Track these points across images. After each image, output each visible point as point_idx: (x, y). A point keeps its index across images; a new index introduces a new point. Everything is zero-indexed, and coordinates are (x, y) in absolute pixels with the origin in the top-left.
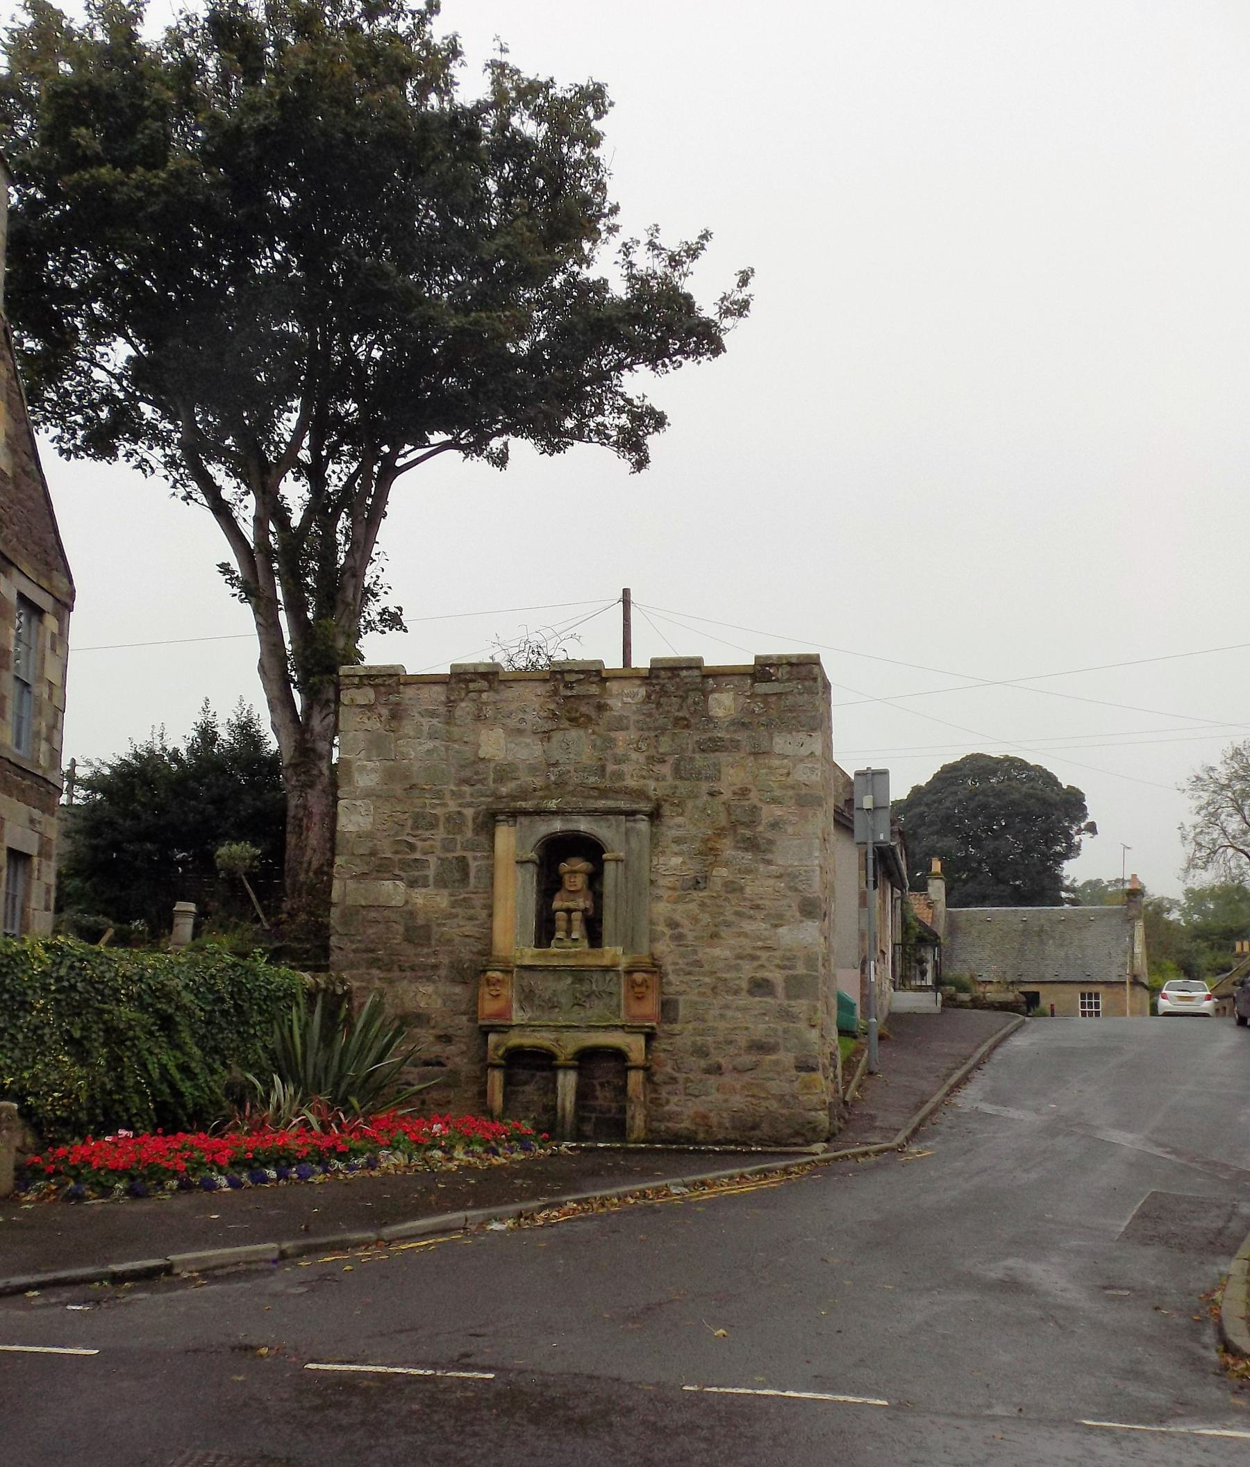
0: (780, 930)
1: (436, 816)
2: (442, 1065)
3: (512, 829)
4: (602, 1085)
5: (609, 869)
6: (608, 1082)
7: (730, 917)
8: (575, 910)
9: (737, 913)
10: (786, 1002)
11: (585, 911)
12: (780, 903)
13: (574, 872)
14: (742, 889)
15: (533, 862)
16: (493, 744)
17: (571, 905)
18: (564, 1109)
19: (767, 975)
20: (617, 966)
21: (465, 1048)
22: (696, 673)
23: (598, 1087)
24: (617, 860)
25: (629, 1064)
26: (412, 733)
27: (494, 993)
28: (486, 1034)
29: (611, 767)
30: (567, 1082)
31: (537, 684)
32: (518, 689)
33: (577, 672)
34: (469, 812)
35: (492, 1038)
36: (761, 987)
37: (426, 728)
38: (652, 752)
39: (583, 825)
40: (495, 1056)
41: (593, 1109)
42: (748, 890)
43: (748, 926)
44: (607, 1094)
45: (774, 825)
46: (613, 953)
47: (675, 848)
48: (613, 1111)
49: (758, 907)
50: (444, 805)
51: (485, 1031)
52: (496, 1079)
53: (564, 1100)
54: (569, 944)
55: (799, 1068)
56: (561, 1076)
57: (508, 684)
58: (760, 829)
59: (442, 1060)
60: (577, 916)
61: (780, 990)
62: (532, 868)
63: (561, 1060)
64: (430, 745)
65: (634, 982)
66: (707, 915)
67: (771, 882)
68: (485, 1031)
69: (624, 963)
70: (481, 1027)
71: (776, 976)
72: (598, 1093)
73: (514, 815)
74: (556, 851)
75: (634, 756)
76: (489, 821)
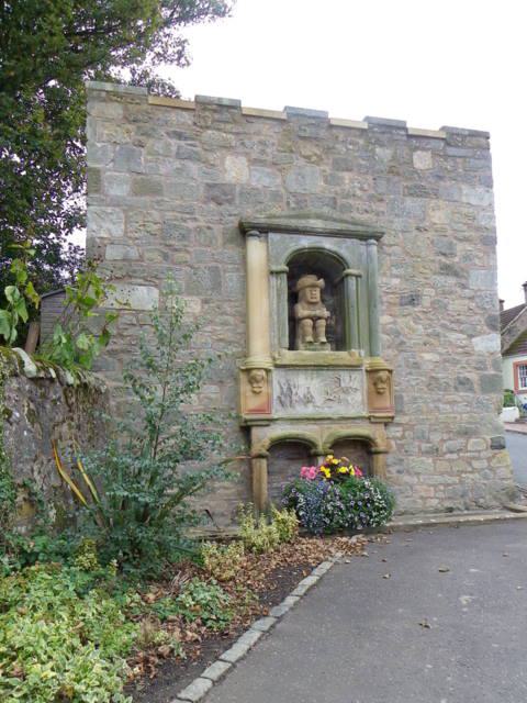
0: (474, 340)
1: (189, 230)
5: (352, 282)
7: (439, 329)
8: (320, 318)
9: (443, 326)
10: (481, 397)
12: (472, 319)
13: (314, 286)
14: (445, 307)
15: (283, 272)
16: (235, 170)
17: (318, 313)
19: (467, 375)
22: (403, 133)
24: (357, 276)
25: (373, 449)
26: (161, 152)
27: (257, 390)
29: (340, 201)
31: (275, 123)
32: (257, 126)
33: (310, 117)
34: (218, 229)
35: (256, 432)
36: (463, 383)
37: (174, 149)
38: (372, 192)
39: (328, 244)
42: (450, 307)
43: (453, 336)
45: (467, 257)
46: (356, 354)
47: (395, 271)
49: (458, 321)
50: (195, 219)
51: (246, 430)
54: (319, 347)
55: (493, 447)
57: (248, 119)
58: (456, 259)
60: (322, 323)
61: (476, 387)
62: (285, 276)
63: (320, 449)
64: (177, 164)
66: (420, 327)
67: (467, 302)
69: (367, 363)
71: (474, 376)
73: (264, 230)
74: (302, 265)
75: (359, 193)
76: (244, 231)
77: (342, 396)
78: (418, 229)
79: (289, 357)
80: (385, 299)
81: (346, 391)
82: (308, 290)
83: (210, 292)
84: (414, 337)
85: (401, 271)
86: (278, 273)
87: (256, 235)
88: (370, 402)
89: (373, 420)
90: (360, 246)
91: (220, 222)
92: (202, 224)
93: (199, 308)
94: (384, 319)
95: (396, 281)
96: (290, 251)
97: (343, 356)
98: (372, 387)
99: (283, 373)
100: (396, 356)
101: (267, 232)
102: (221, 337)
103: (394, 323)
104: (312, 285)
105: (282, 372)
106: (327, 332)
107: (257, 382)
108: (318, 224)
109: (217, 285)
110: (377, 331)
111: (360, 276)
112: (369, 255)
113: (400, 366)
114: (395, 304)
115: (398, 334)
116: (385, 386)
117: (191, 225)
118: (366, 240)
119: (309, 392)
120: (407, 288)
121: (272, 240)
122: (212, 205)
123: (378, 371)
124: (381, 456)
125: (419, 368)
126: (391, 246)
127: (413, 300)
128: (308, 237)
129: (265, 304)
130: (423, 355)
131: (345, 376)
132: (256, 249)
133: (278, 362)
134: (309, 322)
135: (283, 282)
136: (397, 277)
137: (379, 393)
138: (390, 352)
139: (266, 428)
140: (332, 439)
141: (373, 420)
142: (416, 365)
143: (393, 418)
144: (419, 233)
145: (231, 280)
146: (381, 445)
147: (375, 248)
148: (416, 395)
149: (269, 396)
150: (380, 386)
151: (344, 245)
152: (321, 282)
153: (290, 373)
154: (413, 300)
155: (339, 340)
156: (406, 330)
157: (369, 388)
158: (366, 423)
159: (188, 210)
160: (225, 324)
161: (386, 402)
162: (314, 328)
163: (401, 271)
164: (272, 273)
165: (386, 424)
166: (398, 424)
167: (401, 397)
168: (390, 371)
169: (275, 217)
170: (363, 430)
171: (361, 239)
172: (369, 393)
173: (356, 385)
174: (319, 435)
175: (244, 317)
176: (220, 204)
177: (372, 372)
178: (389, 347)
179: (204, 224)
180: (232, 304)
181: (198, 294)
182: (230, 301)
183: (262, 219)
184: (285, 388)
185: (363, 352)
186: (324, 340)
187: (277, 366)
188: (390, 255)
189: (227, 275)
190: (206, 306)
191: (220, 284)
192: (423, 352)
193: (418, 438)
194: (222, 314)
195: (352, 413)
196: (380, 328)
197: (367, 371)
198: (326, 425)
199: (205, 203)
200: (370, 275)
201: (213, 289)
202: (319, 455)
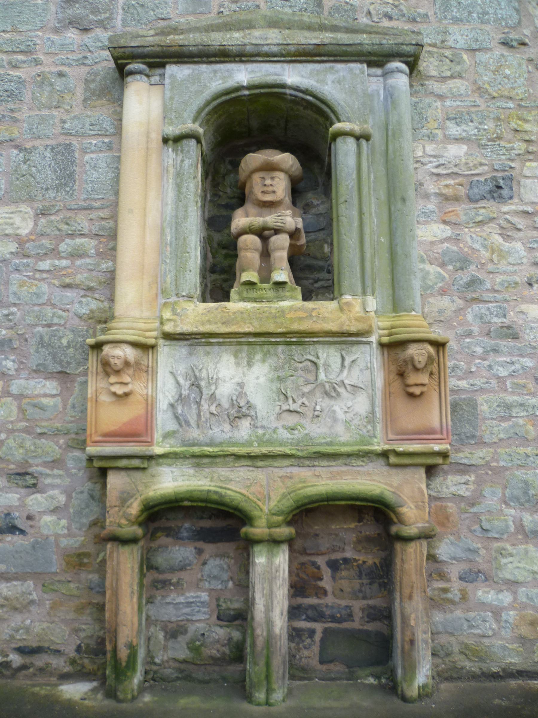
2: (13, 529)
3: (156, 91)
4: (334, 565)
5: (345, 154)
6: (346, 561)
11: (294, 234)
13: (270, 168)
17: (270, 219)
18: (269, 623)
20: (367, 333)
21: (62, 499)
23: (326, 572)
24: (362, 137)
27: (120, 390)
28: (103, 472)
30: (272, 567)
34: (76, 75)
35: (115, 481)
39: (294, 76)
40: (124, 517)
41: (318, 615)
44: (345, 584)
46: (358, 306)
47: (454, 130)
48: (358, 614)
51: (100, 470)
52: (126, 564)
53: (269, 609)
56: (260, 559)
59: (19, 523)
60: (281, 243)
63: (259, 529)
65: (411, 363)
66: (518, 245)
68: (100, 470)
69: (381, 326)
70: (90, 459)
72: (326, 583)
77: (323, 403)
78: (505, 44)
79: (197, 314)
80: (431, 187)
81: (331, 392)
82: (256, 177)
83: (51, 194)
84: (503, 266)
85: (471, 129)
86: (178, 139)
87: (140, 72)
88: (390, 416)
89: (393, 459)
90: (372, 81)
91: (82, 62)
92: (49, 67)
93: (31, 224)
94: (430, 232)
95: (456, 152)
96: (207, 94)
97: (325, 313)
98: (397, 385)
99: (184, 351)
100: (459, 311)
101: (163, 65)
102: (67, 281)
103: (456, 239)
104: (271, 172)
105: (181, 350)
106: (292, 261)
107: (118, 372)
108: (272, 38)
109: (66, 178)
110: (407, 256)
111: (367, 138)
112: (390, 95)
113: (469, 334)
114: (456, 199)
115: (463, 262)
116: (424, 378)
117: (25, 73)
118: (380, 64)
119: (242, 394)
120: (483, 164)
121: (172, 76)
122: (72, 35)
123: (403, 344)
124: (412, 548)
125: (515, 337)
126: (444, 79)
127: (498, 189)
128: (250, 66)
129: (157, 205)
130: (524, 307)
131: (328, 356)
132: (144, 104)
133: (169, 328)
134: (252, 240)
135: (191, 159)
136: (458, 140)
137: (411, 395)
138: (445, 302)
139: (138, 475)
140: (288, 503)
141: (393, 459)
142: (510, 333)
143: (444, 455)
144: (505, 51)
145: (93, 166)
146: (413, 515)
147: (401, 81)
148: (510, 399)
149: (150, 406)
150: (413, 378)
151: (330, 77)
152: (287, 159)
153: (201, 350)
154: (498, 189)
155: (314, 273)
156: (485, 254)
157: (388, 384)
158: (377, 468)
159: (22, 47)
160: (76, 254)
161: (433, 414)
162: (266, 254)
163: (471, 129)
164: (165, 141)
165: (431, 470)
166: (464, 469)
167: (473, 405)
168: (439, 345)
169: (175, 30)
170: (367, 481)
171: (370, 64)
172: (388, 394)
173: (353, 377)
174: (263, 492)
175: (109, 239)
176: (86, 30)
177: (393, 347)
178: (443, 292)
179: (54, 69)
180: (94, 215)
181: (30, 199)
182: (89, 208)
183: (148, 37)
184: (185, 384)
185: (372, 303)
186: (282, 274)
187: (168, 337)
188: (441, 97)
189: (87, 157)
190: (43, 221)
191: (71, 176)
192: (525, 300)
193: (516, 499)
194: (72, 236)
195: (344, 438)
196: (416, 252)
197: (382, 345)
198: (280, 470)
199: (56, 31)
200: (390, 133)
201: (58, 188)
202: (258, 542)
